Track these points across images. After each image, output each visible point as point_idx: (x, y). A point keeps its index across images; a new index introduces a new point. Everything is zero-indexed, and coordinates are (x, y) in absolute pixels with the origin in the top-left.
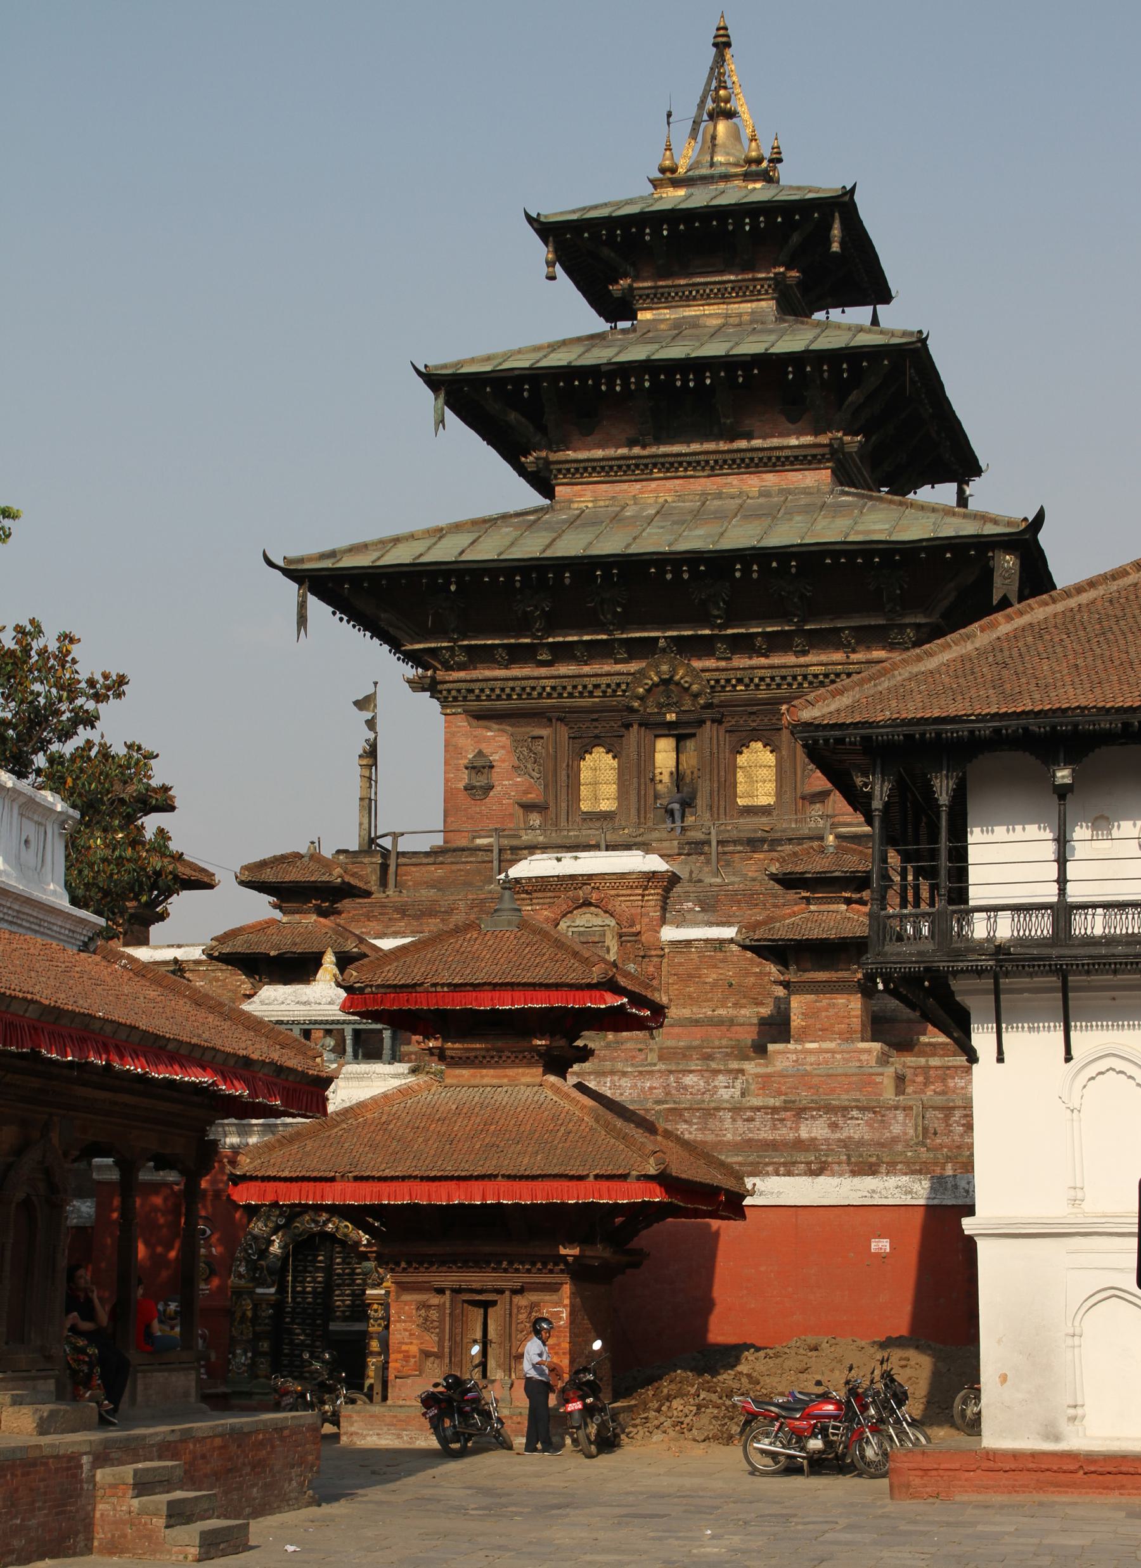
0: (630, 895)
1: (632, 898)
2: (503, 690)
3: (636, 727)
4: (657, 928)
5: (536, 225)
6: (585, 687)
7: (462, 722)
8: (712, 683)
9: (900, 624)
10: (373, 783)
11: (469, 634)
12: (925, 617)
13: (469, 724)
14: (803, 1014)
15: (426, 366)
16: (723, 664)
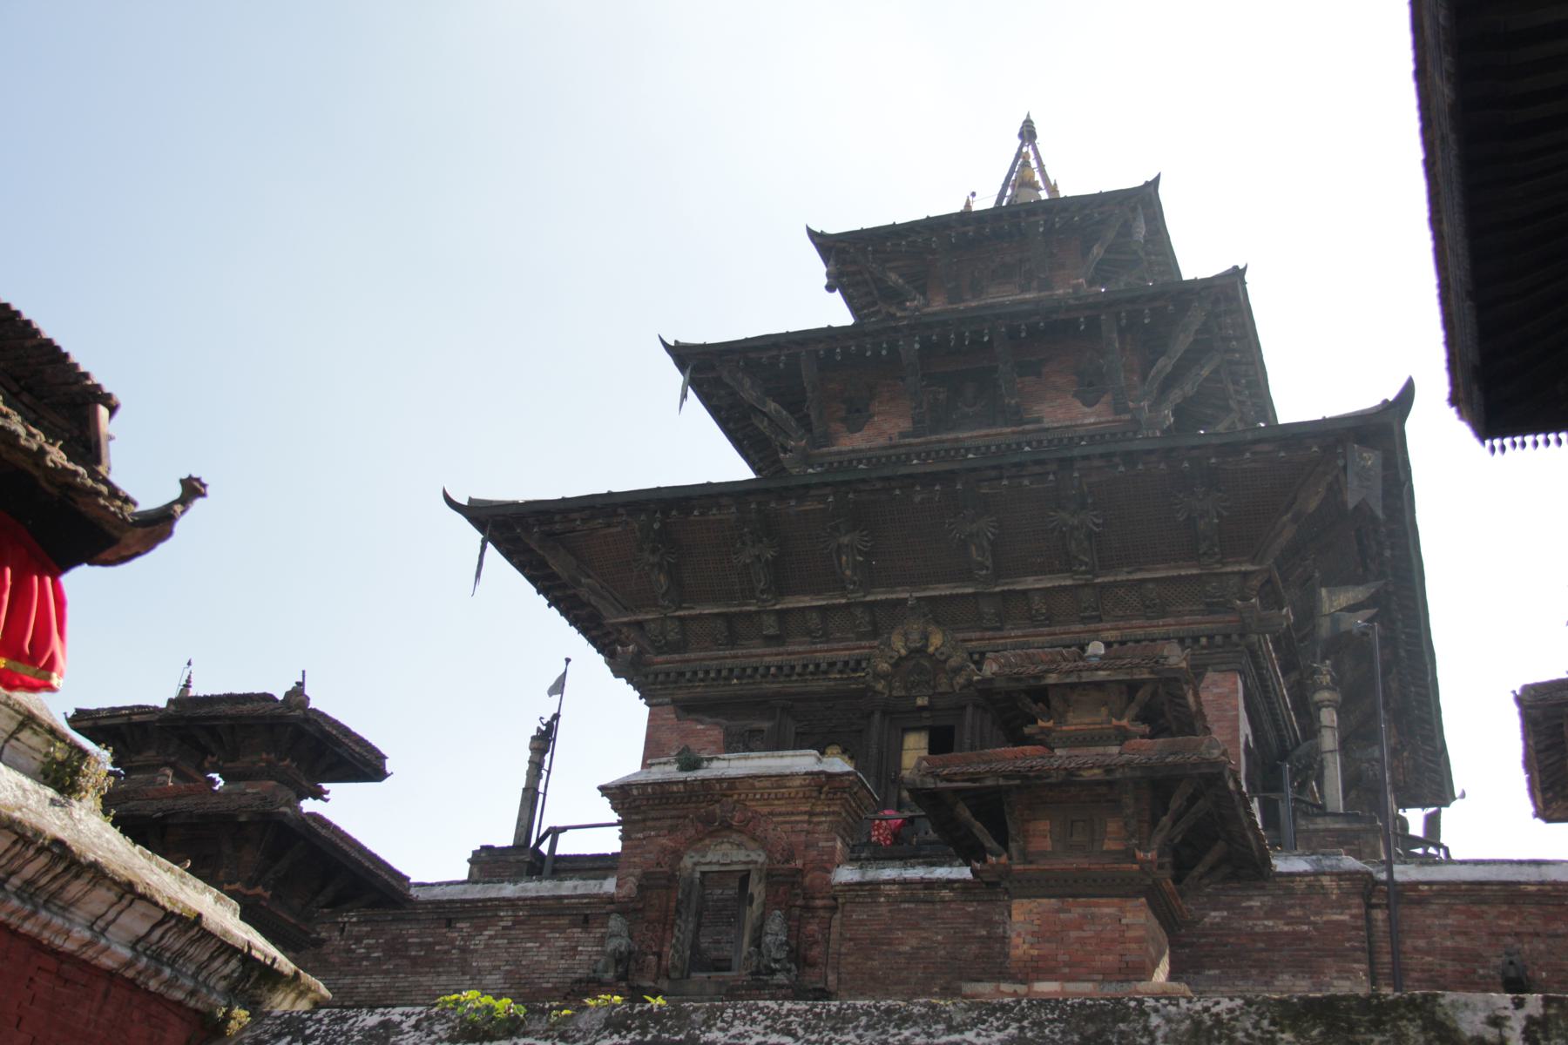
0: (793, 814)
1: (793, 818)
2: (719, 671)
3: (877, 716)
4: (828, 866)
5: (816, 239)
6: (817, 666)
7: (669, 715)
8: (976, 657)
9: (1216, 574)
10: (544, 773)
11: (684, 605)
12: (1253, 564)
13: (677, 717)
14: (1033, 934)
15: (676, 342)
16: (988, 634)
